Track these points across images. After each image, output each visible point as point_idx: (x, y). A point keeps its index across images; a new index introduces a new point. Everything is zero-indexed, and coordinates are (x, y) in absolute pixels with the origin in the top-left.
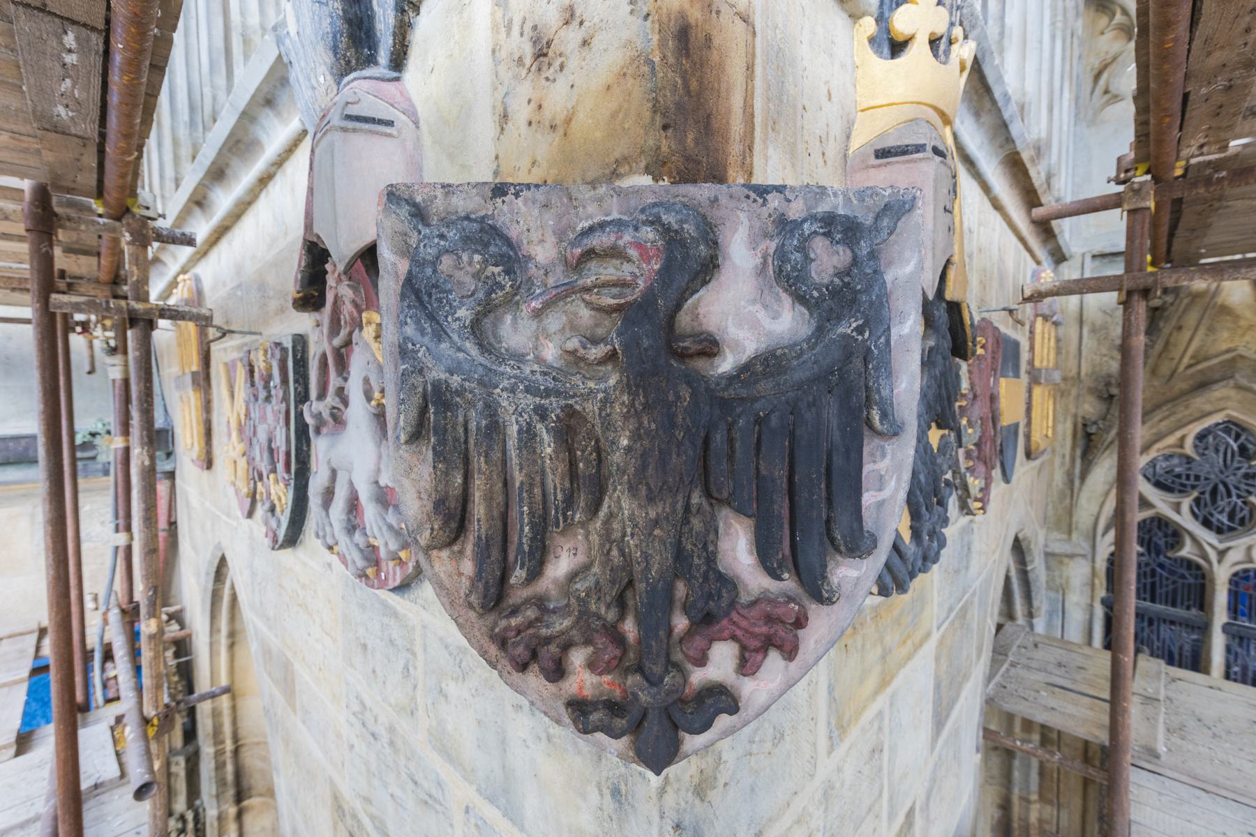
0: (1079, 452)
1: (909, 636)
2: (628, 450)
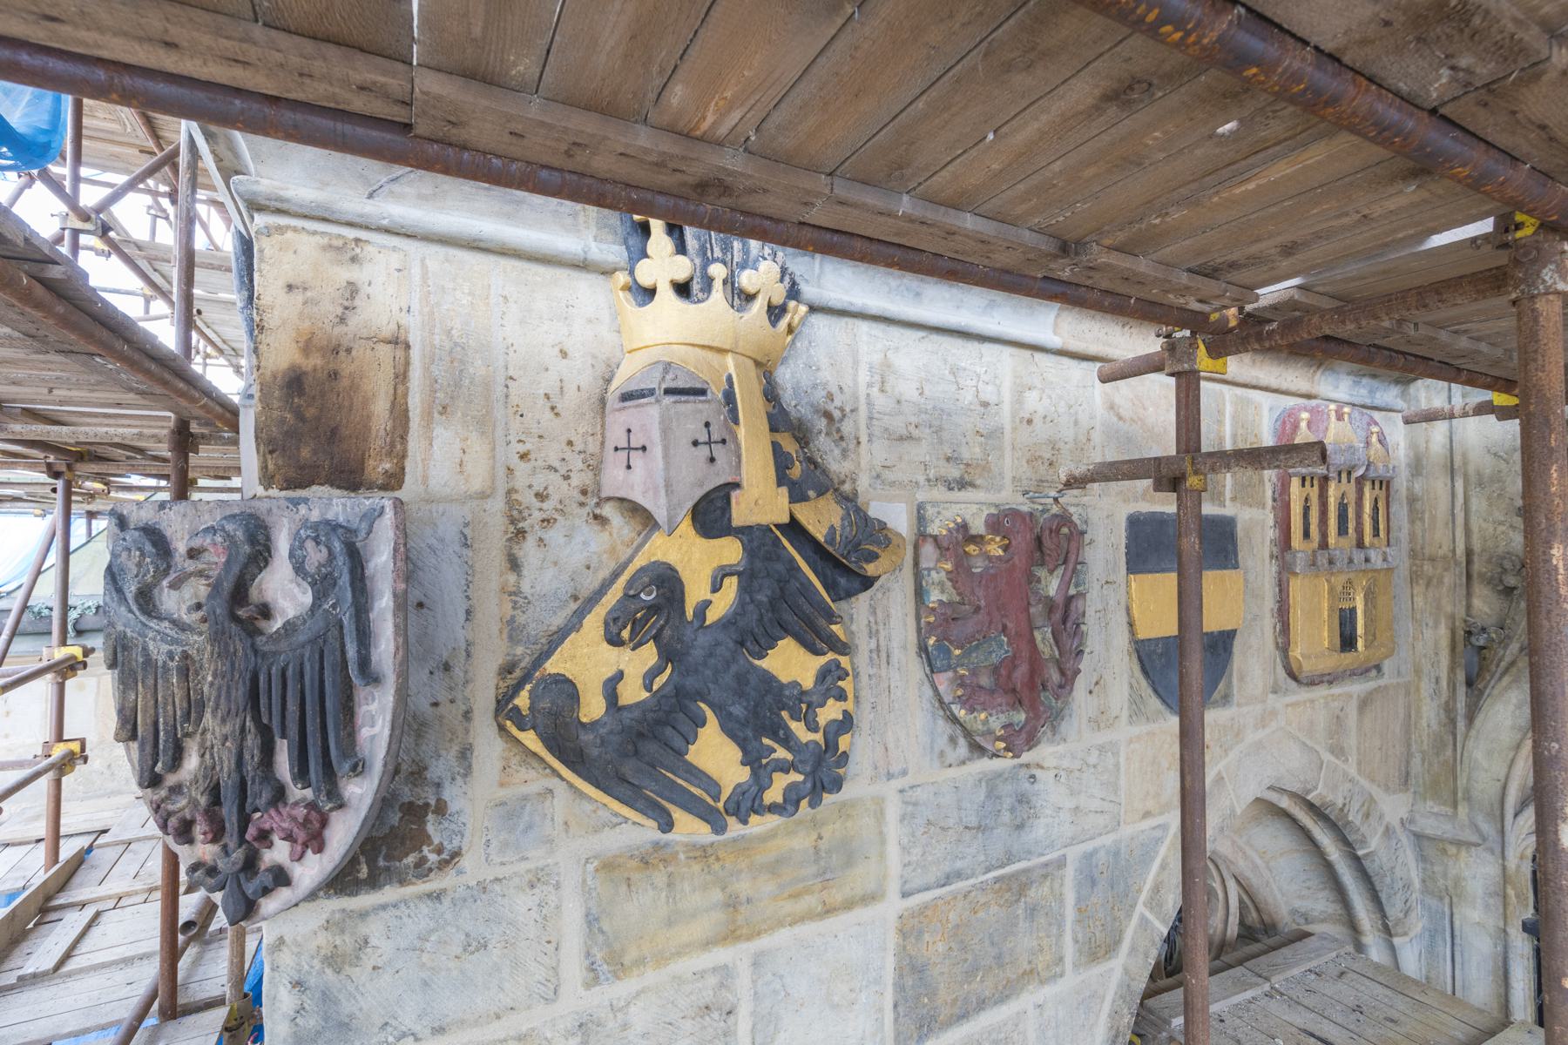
0: (1461, 676)
1: (807, 891)
2: (212, 684)
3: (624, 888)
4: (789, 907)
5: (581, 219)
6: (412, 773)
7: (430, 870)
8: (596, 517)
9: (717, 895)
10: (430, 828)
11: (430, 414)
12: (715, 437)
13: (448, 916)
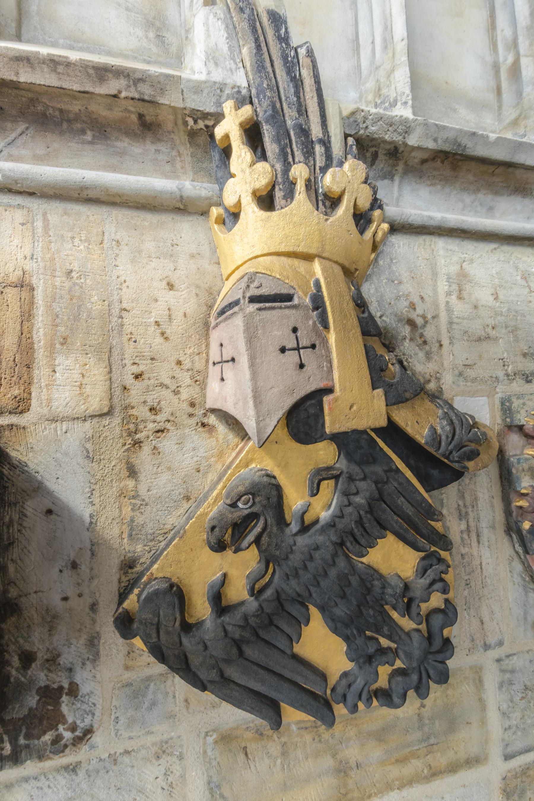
1: (414, 755)
3: (242, 756)
4: (395, 772)
5: (178, 165)
6: (47, 661)
7: (66, 746)
8: (203, 425)
9: (328, 762)
10: (64, 709)
11: (52, 346)
12: (304, 342)
13: (84, 786)
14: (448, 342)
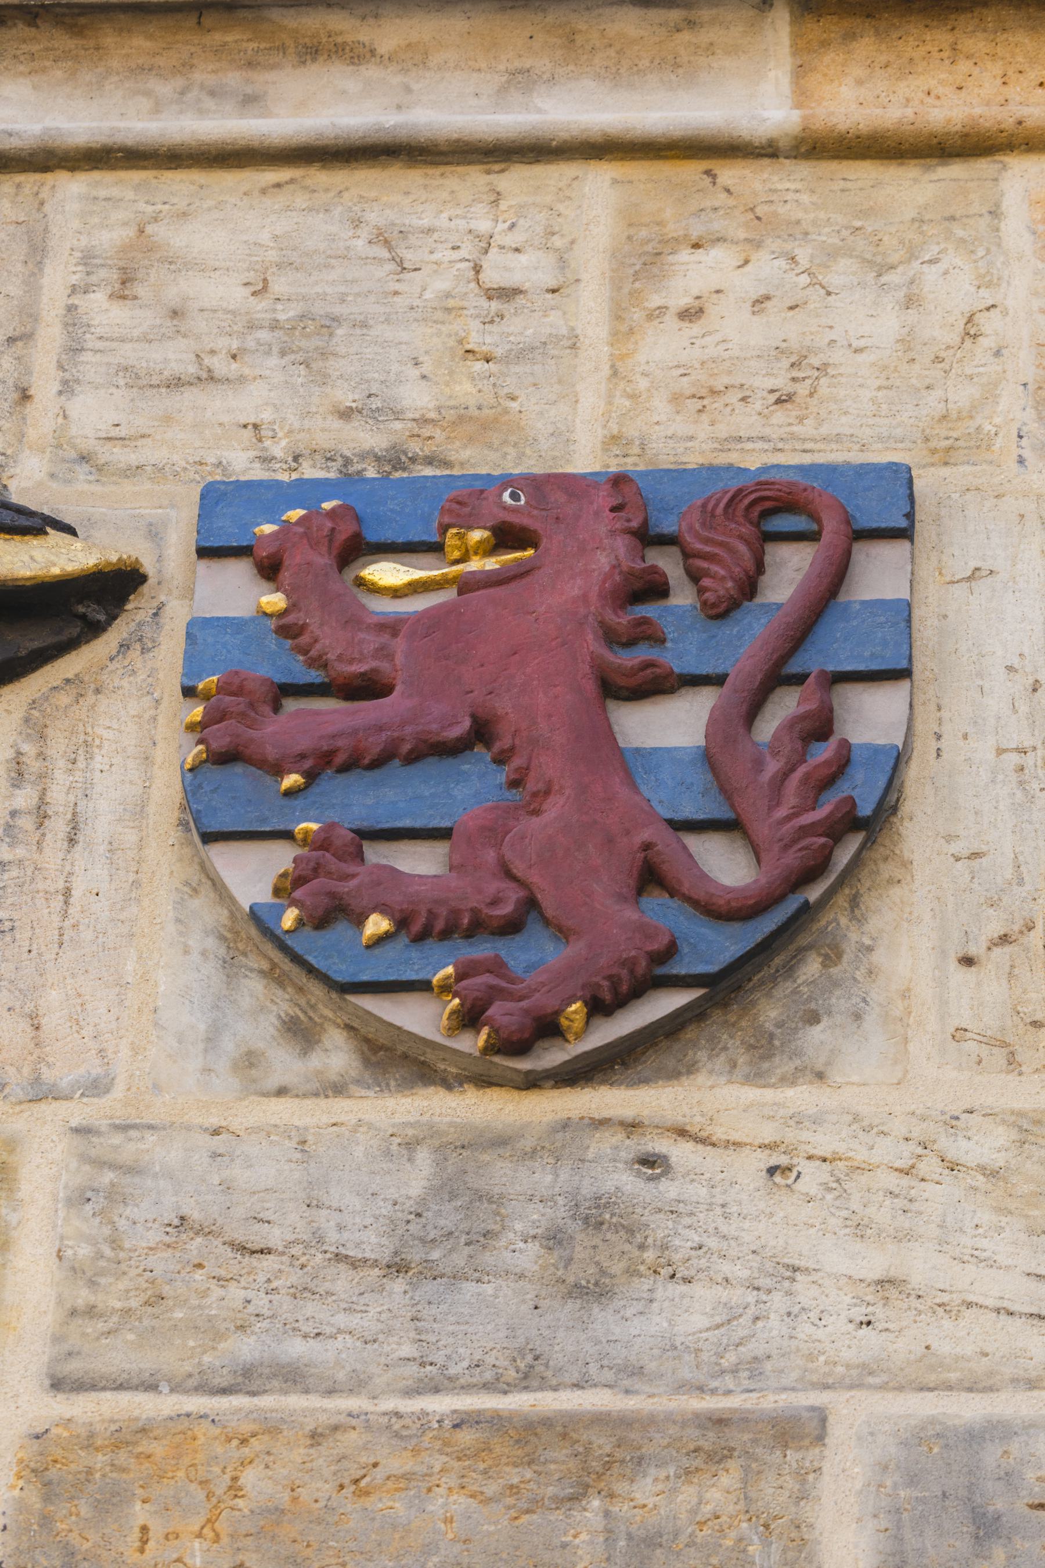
14: (56, 387)
